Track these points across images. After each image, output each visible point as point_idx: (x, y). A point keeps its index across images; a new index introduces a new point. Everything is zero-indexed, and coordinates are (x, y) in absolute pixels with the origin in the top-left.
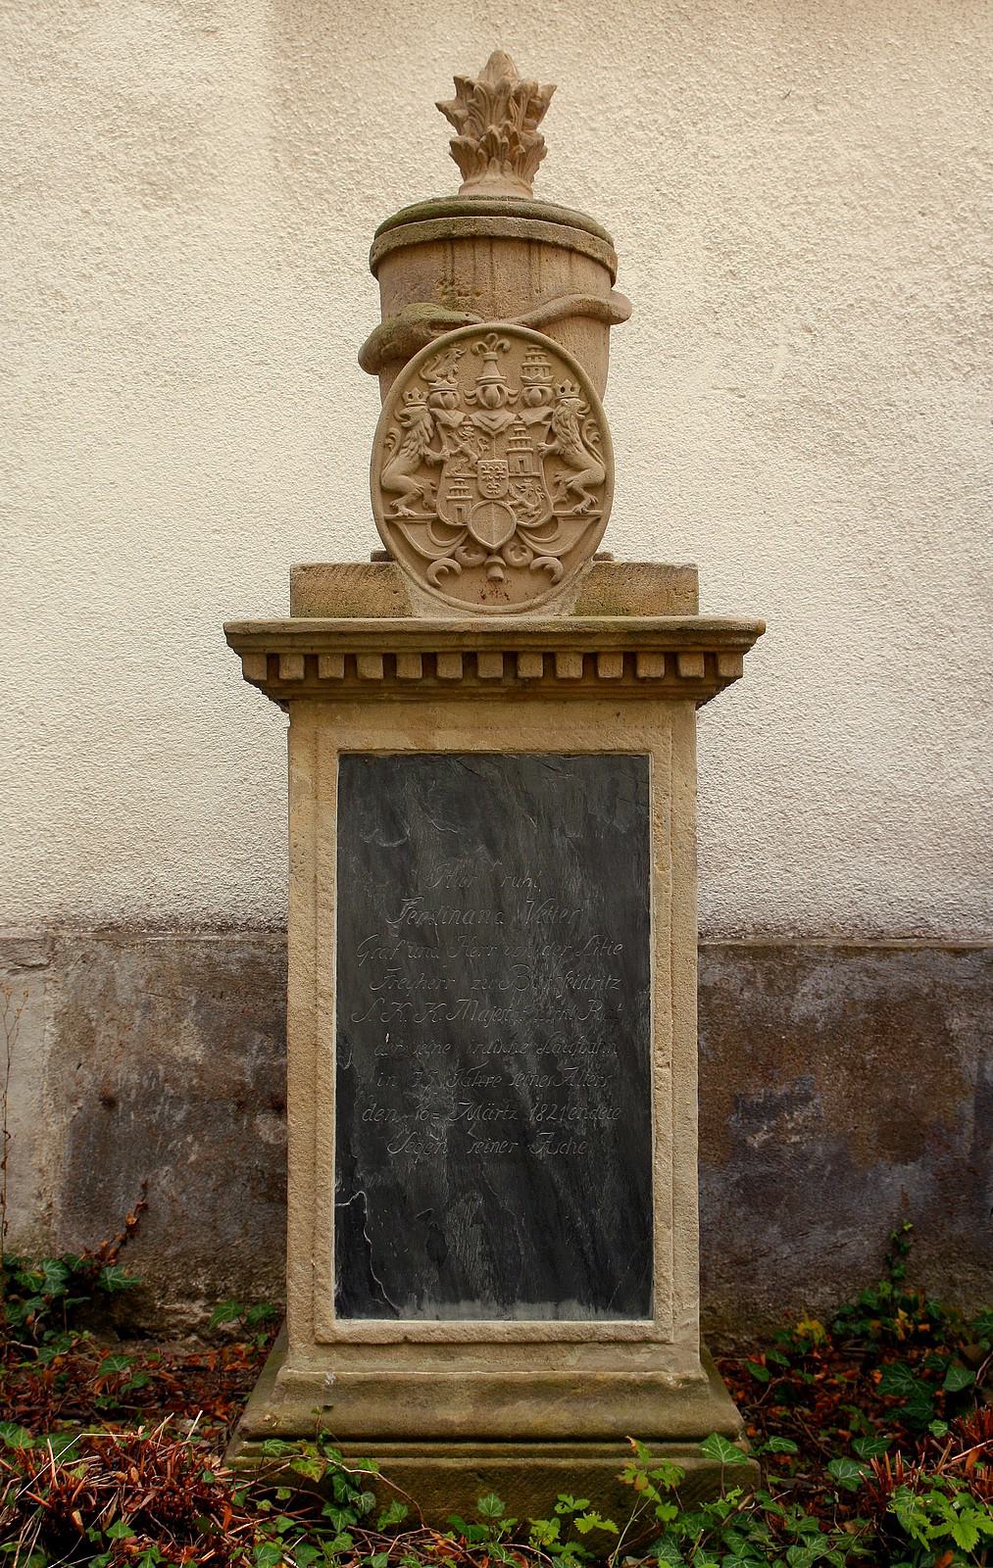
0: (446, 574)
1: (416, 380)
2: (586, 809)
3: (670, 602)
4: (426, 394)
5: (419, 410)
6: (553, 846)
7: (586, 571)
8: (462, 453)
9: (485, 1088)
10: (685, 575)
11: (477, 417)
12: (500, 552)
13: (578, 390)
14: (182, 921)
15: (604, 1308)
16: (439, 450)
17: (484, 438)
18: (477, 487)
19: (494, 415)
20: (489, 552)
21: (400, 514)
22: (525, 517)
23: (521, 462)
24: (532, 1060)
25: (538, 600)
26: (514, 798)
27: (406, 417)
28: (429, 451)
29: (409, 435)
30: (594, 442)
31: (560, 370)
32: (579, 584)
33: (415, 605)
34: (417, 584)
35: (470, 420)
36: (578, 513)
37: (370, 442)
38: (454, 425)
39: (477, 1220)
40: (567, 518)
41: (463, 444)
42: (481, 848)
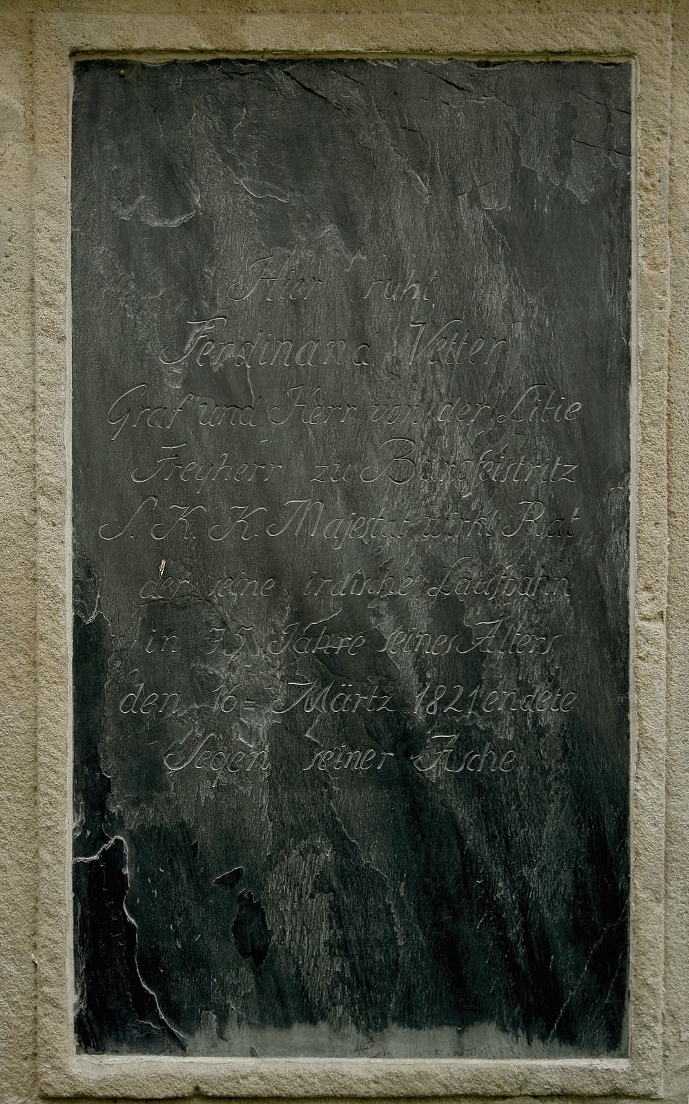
2: (516, 160)
6: (457, 227)
9: (335, 658)
15: (543, 1038)
24: (419, 608)
26: (388, 140)
39: (322, 885)
42: (329, 230)
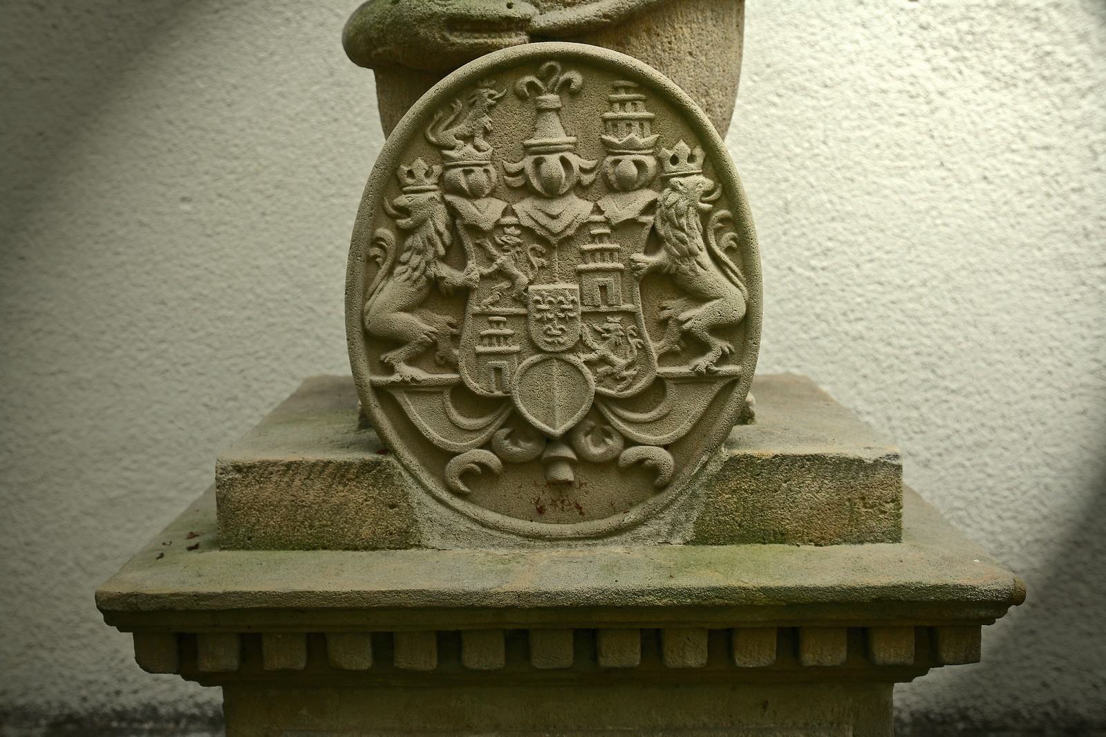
0: (477, 476)
1: (419, 146)
3: (854, 520)
4: (437, 169)
5: (423, 194)
7: (713, 468)
8: (502, 274)
10: (880, 475)
11: (525, 208)
12: (568, 438)
13: (700, 160)
14: (163, 711)
16: (462, 266)
17: (539, 247)
18: (527, 330)
19: (555, 207)
20: (548, 440)
21: (395, 378)
22: (608, 381)
23: (603, 288)
25: (632, 516)
27: (405, 211)
28: (444, 270)
29: (409, 242)
30: (729, 250)
31: (669, 125)
32: (701, 492)
33: (425, 528)
34: (429, 492)
35: (514, 214)
36: (699, 374)
37: (344, 255)
38: (487, 226)
40: (681, 380)
41: (502, 259)
